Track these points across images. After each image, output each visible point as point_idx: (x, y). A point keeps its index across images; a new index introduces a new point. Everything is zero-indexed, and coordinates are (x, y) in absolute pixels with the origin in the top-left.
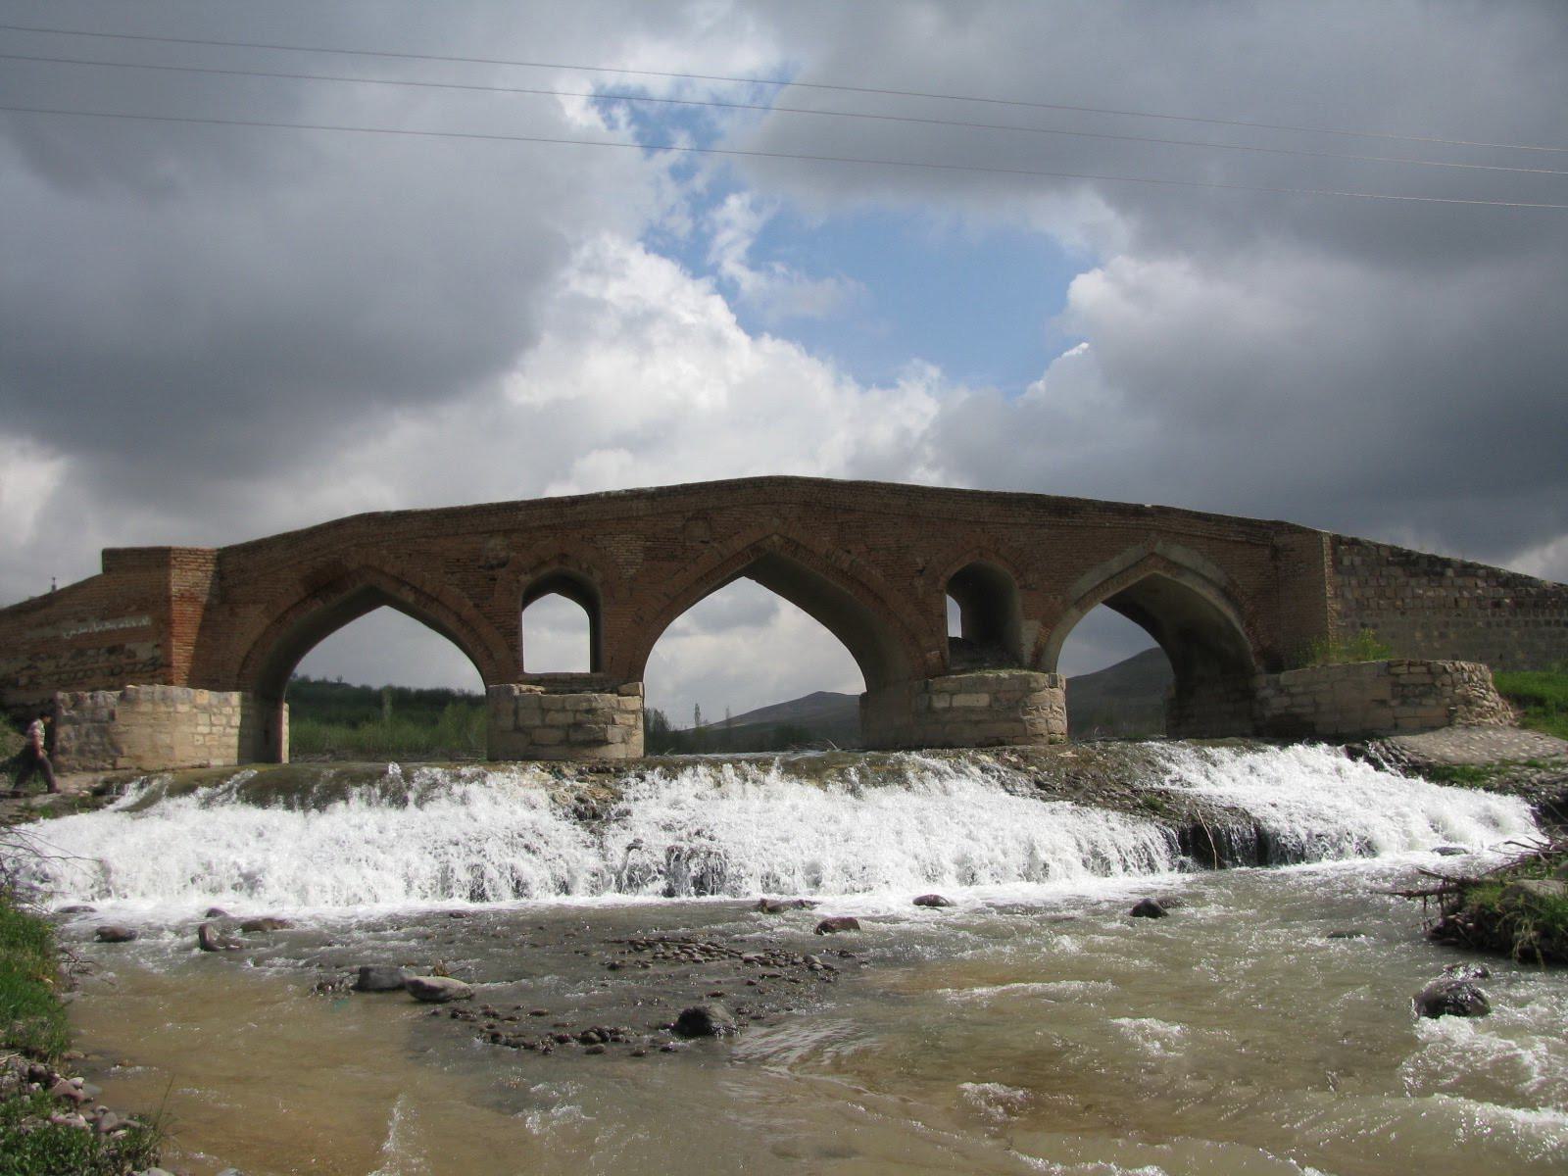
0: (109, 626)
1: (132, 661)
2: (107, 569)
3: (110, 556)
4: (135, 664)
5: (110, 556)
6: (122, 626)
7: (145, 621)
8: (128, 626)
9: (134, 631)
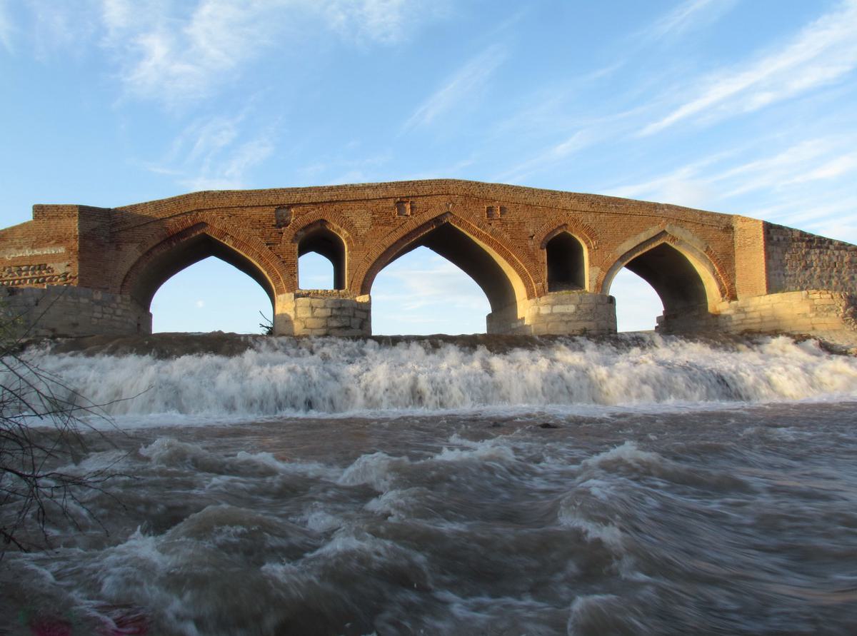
0: (37, 252)
1: (51, 274)
2: (36, 217)
3: (40, 211)
4: (53, 276)
5: (40, 211)
6: (45, 252)
7: (62, 250)
8: (49, 253)
9: (53, 256)
